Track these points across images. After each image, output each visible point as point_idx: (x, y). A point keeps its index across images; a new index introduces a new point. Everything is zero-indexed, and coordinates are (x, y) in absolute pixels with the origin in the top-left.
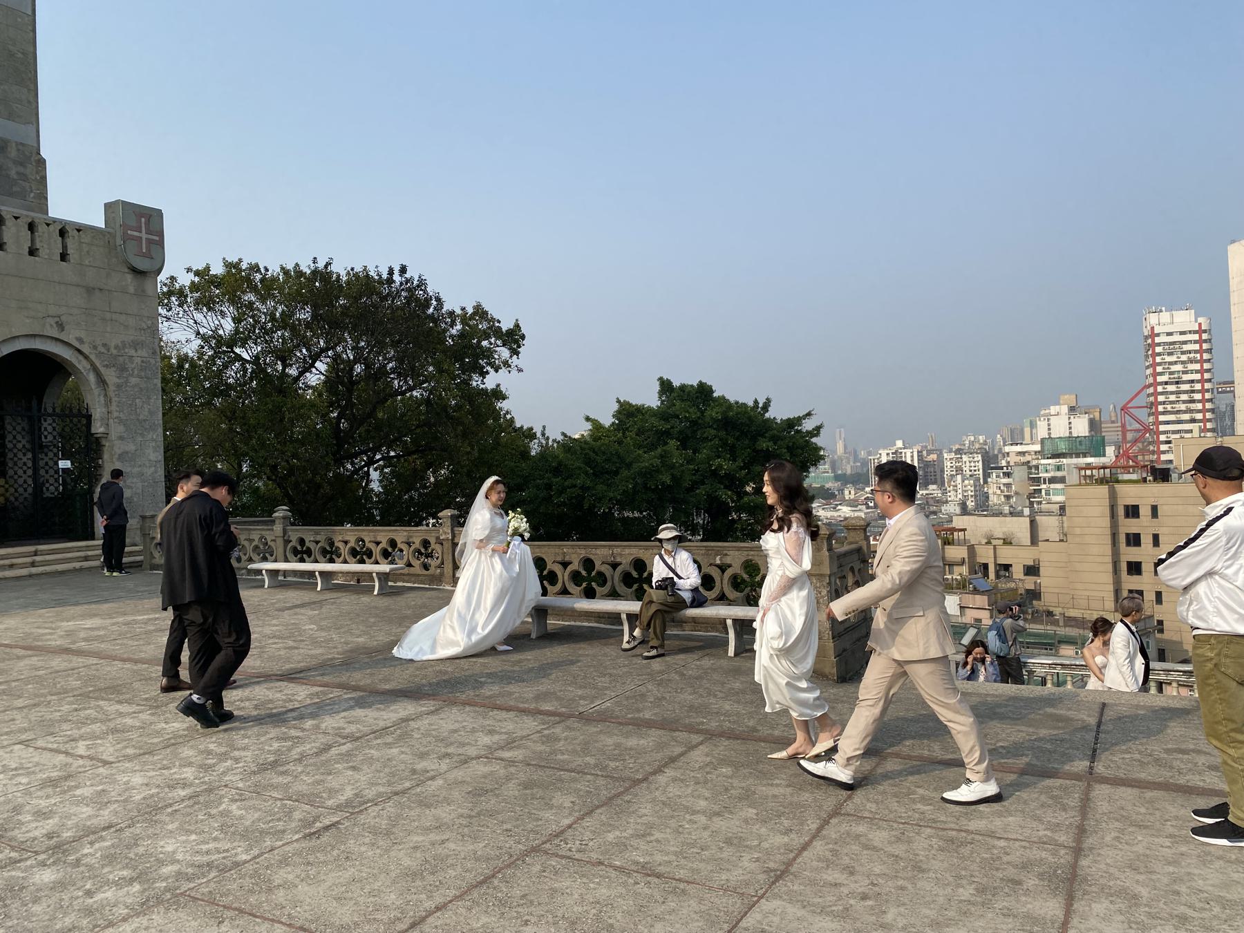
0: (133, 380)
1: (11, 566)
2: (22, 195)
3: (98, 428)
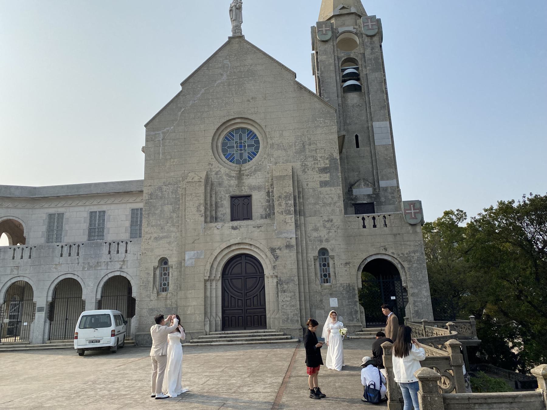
0: (415, 265)
1: (371, 334)
2: (393, 204)
3: (404, 285)
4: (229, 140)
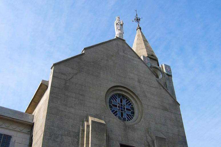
4: (113, 100)
